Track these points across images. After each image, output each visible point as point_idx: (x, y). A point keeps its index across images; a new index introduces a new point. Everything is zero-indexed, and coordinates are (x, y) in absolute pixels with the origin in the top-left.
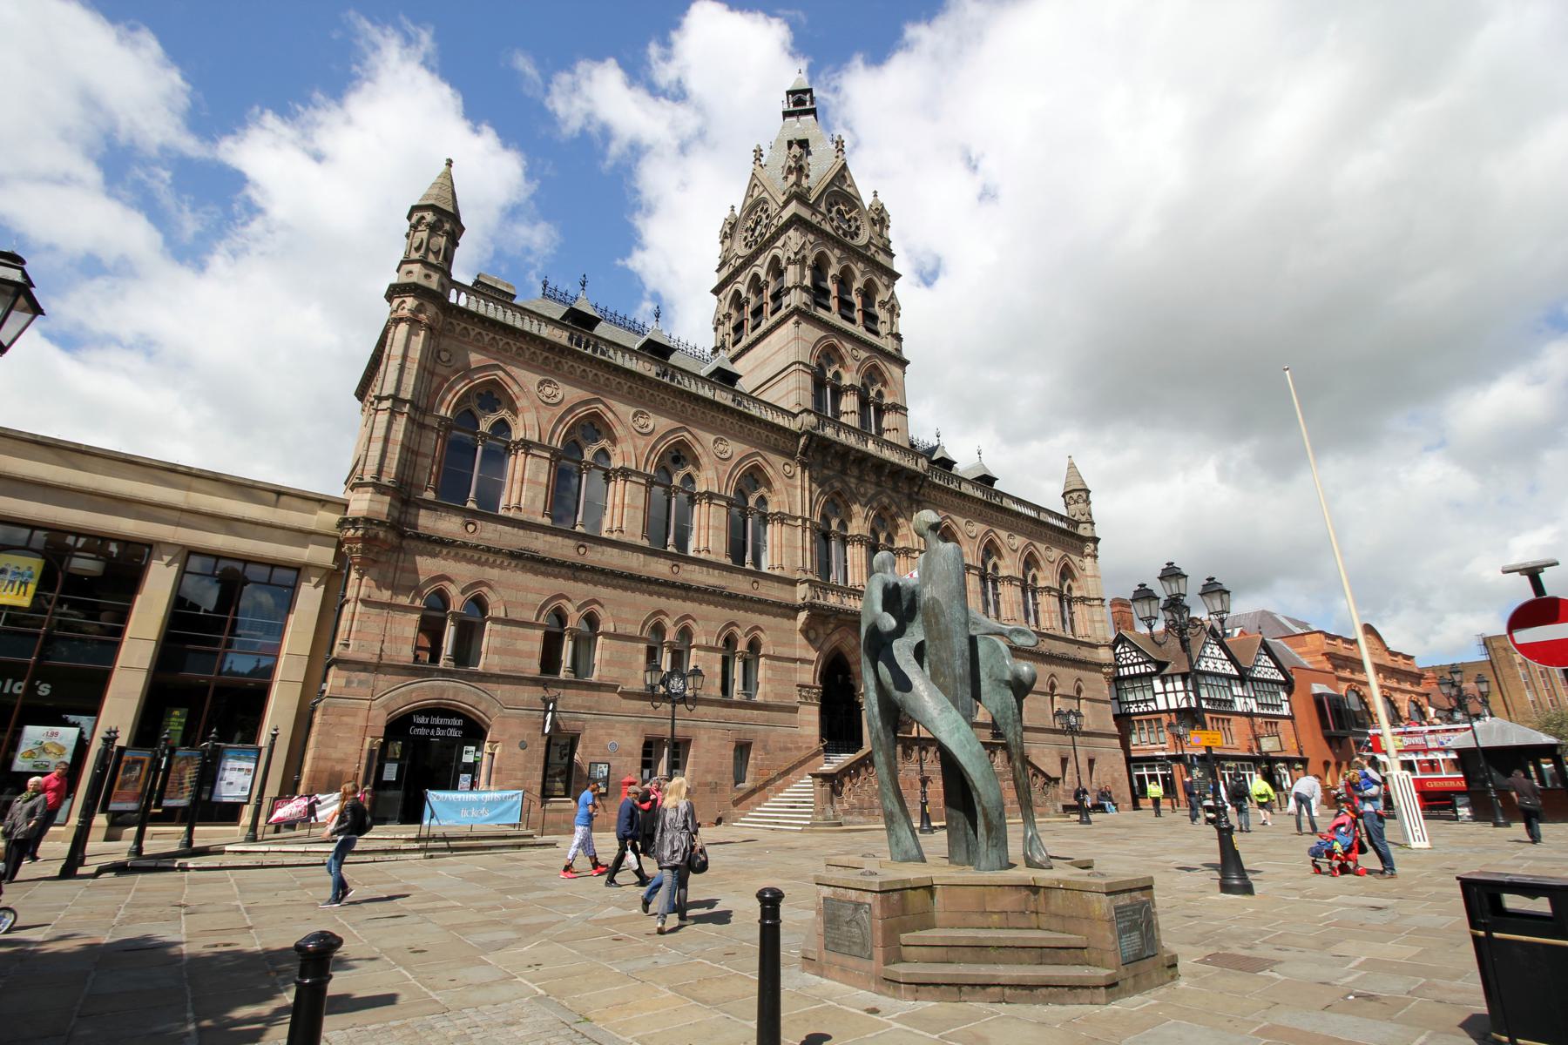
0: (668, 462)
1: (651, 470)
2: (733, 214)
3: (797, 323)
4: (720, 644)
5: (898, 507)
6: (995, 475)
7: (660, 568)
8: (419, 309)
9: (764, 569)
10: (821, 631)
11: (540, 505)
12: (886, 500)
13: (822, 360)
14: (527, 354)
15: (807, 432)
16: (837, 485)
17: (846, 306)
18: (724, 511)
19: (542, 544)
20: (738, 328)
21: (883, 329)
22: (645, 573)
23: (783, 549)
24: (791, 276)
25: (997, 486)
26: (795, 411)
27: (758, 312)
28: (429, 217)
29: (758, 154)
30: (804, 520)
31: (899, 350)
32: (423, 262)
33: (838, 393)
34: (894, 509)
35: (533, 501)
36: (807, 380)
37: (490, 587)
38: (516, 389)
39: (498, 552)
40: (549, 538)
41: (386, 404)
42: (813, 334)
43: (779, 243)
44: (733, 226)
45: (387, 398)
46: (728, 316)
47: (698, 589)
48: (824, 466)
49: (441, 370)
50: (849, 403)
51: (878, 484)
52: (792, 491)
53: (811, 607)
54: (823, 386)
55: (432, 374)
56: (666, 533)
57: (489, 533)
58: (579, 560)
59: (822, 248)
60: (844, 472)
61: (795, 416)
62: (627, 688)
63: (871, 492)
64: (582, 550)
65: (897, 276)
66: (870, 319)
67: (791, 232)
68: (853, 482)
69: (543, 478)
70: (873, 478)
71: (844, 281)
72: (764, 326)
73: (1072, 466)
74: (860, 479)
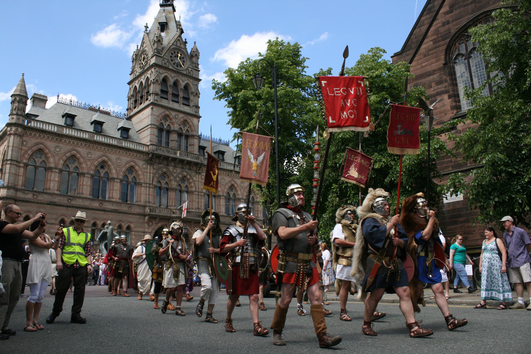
0: (99, 168)
2: (137, 49)
3: (152, 108)
5: (190, 176)
8: (17, 130)
9: (134, 203)
10: (154, 222)
11: (56, 188)
12: (185, 174)
13: (163, 121)
14: (50, 138)
15: (151, 153)
16: (164, 170)
17: (176, 96)
18: (119, 184)
19: (56, 200)
20: (136, 101)
21: (192, 104)
22: (90, 207)
23: (143, 195)
24: (152, 89)
26: (148, 144)
27: (142, 97)
28: (18, 99)
29: (147, 27)
30: (150, 184)
31: (198, 112)
32: (17, 114)
33: (169, 132)
34: (188, 177)
35: (54, 186)
36: (155, 131)
38: (47, 151)
39: (44, 204)
40: (59, 198)
41: (9, 162)
42: (158, 111)
43: (149, 72)
44: (136, 55)
45: (9, 160)
46: (132, 96)
47: (108, 211)
48: (160, 163)
49: (24, 148)
50: (174, 137)
52: (146, 173)
53: (149, 215)
54: (162, 131)
55: (21, 149)
56: (98, 193)
57: (41, 198)
59: (166, 74)
60: (168, 165)
61: (148, 146)
63: (179, 171)
64: (70, 201)
65: (200, 80)
66: (187, 99)
67: (153, 70)
68: (171, 168)
69: (57, 179)
70: (180, 166)
71: (176, 84)
72: (142, 106)
74: (175, 167)
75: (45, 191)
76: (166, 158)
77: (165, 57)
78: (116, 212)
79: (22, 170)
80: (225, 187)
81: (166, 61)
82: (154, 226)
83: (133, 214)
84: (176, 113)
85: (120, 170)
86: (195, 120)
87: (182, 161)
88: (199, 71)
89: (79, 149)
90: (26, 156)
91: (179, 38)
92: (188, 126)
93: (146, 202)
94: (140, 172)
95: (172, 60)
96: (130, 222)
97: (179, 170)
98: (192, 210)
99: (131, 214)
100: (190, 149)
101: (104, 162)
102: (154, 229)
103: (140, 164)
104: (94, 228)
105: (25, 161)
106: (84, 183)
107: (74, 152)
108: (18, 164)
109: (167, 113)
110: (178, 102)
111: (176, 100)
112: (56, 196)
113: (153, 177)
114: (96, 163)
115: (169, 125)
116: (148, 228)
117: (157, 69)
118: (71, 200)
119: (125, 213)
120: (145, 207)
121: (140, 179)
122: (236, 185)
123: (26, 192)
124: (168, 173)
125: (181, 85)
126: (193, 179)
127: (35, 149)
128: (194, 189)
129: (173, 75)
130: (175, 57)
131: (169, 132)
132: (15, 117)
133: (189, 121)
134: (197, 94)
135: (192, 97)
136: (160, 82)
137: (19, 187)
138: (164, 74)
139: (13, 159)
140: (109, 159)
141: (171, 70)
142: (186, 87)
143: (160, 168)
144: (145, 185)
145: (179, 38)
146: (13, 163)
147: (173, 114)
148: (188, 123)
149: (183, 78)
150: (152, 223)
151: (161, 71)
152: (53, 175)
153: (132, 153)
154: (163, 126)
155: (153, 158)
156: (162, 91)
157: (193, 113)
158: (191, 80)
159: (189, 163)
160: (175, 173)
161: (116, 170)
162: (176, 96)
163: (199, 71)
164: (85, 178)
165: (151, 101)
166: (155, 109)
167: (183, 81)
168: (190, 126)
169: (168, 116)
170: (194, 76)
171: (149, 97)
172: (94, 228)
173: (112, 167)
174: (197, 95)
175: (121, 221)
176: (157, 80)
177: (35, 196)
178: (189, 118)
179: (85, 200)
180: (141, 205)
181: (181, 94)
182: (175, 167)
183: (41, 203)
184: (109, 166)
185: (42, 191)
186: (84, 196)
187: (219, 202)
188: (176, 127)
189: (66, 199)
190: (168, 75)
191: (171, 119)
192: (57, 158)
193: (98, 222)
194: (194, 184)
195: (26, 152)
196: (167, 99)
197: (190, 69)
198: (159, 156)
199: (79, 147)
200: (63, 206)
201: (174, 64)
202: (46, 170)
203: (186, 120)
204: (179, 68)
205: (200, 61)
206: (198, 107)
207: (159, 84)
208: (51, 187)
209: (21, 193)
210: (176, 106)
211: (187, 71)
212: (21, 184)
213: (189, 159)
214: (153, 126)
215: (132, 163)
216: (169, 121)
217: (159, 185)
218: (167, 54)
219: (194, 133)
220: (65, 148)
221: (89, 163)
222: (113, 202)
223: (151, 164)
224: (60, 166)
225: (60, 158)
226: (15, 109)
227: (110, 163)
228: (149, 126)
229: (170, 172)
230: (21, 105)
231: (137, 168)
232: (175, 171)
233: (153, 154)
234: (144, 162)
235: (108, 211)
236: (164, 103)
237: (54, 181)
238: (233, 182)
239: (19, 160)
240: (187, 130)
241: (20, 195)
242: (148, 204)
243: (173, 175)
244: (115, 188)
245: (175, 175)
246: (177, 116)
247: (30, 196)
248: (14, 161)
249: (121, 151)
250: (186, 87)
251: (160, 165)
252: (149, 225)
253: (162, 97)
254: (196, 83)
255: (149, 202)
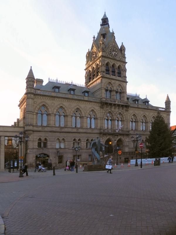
1: (71, 114)
3: (102, 80)
4: (86, 141)
6: (149, 100)
7: (75, 130)
12: (120, 112)
16: (110, 110)
19: (54, 129)
21: (122, 76)
22: (72, 131)
25: (149, 103)
30: (103, 118)
33: (111, 91)
37: (47, 137)
42: (105, 80)
51: (119, 109)
58: (60, 131)
60: (111, 108)
62: (70, 149)
65: (126, 63)
67: (101, 59)
68: (113, 109)
69: (53, 119)
70: (118, 108)
71: (113, 66)
73: (168, 95)
74: (115, 108)
75: (48, 125)
76: (111, 104)
77: (107, 52)
78: (86, 133)
79: (35, 116)
80: (141, 117)
81: (108, 54)
82: (105, 138)
83: (94, 133)
84: (115, 81)
85: (86, 112)
86: (124, 84)
87: (119, 105)
88: (126, 58)
89: (64, 103)
90: (37, 109)
91: (114, 41)
92: (121, 87)
93: (101, 127)
94: (97, 113)
95: (111, 53)
96: (93, 137)
97: (117, 110)
98: (124, 129)
99: (93, 133)
100: (122, 99)
101: (78, 109)
102: (105, 140)
103: (97, 108)
104: (74, 142)
105: (36, 111)
106: (68, 120)
107: (61, 105)
108: (33, 113)
109: (110, 81)
110: (115, 75)
111: (114, 74)
112: (54, 128)
113: (104, 114)
114: (73, 110)
115: (111, 88)
116: (102, 140)
117: (103, 58)
118: (62, 129)
119: (90, 133)
120: (100, 129)
121: (97, 116)
122: (146, 116)
123: (38, 127)
124: (112, 112)
125: (116, 66)
126: (124, 114)
127: (41, 105)
128: (125, 119)
129: (112, 61)
130: (112, 51)
131: (111, 91)
132: (29, 89)
133: (121, 85)
134: (125, 70)
135: (122, 72)
136: (105, 66)
137: (34, 125)
138: (107, 61)
139: (30, 111)
140: (81, 107)
141: (110, 58)
142: (119, 67)
143: (107, 109)
144: (100, 119)
145: (114, 41)
146: (30, 113)
147: (113, 81)
148: (121, 86)
149: (118, 62)
150: (104, 137)
151: (106, 59)
152: (51, 117)
153: (92, 103)
154: (108, 88)
155: (104, 104)
156: (106, 70)
157: (124, 80)
158: (122, 63)
159: (122, 106)
160: (115, 112)
161: (84, 112)
162: (114, 72)
163: (126, 58)
164: (68, 118)
165: (101, 76)
166: (103, 79)
167: (117, 64)
168: (122, 87)
169: (110, 83)
170: (123, 61)
171: (99, 74)
172: (74, 142)
173: (82, 111)
174: (125, 70)
175: (88, 137)
176: (103, 64)
177: (43, 129)
178: (122, 83)
179: (69, 129)
180: (98, 129)
181: (117, 71)
182: (115, 108)
183: (46, 132)
184: (80, 111)
185: (46, 126)
186: (68, 126)
187: (138, 124)
188: (115, 88)
189: (59, 128)
190: (109, 62)
191: (111, 84)
192: (53, 109)
193: (76, 139)
194: (125, 116)
195: (36, 106)
196: (109, 74)
197: (121, 57)
198: (106, 104)
199: (64, 102)
200: (58, 132)
201: (112, 55)
202: (47, 115)
203: (120, 85)
204: (115, 57)
205: (126, 53)
206: (126, 77)
207: (105, 66)
208: (51, 123)
209: (35, 128)
210: (114, 77)
211: (119, 59)
212: (35, 123)
213: (123, 104)
214: (102, 89)
215: (92, 108)
216: (111, 85)
217: (106, 118)
218: (108, 50)
219: (124, 91)
220: (57, 103)
221: (70, 110)
222: (84, 128)
223: (103, 108)
224: (55, 113)
225: (54, 108)
226: (29, 85)
227: (81, 109)
228: (101, 89)
229: (112, 111)
230: (31, 83)
231: (95, 110)
232: (115, 111)
233: (104, 102)
234: (99, 107)
235: (82, 133)
236: (108, 76)
237: (52, 120)
238: (144, 114)
239: (33, 111)
240: (120, 89)
241: (35, 129)
242: (102, 128)
243: (114, 113)
244: (84, 121)
245: (115, 112)
246: (115, 83)
247: (40, 129)
248: (28, 111)
249: (87, 103)
250: (119, 67)
251: (107, 108)
252: (102, 138)
253: (106, 73)
254: (124, 64)
255: (103, 127)
